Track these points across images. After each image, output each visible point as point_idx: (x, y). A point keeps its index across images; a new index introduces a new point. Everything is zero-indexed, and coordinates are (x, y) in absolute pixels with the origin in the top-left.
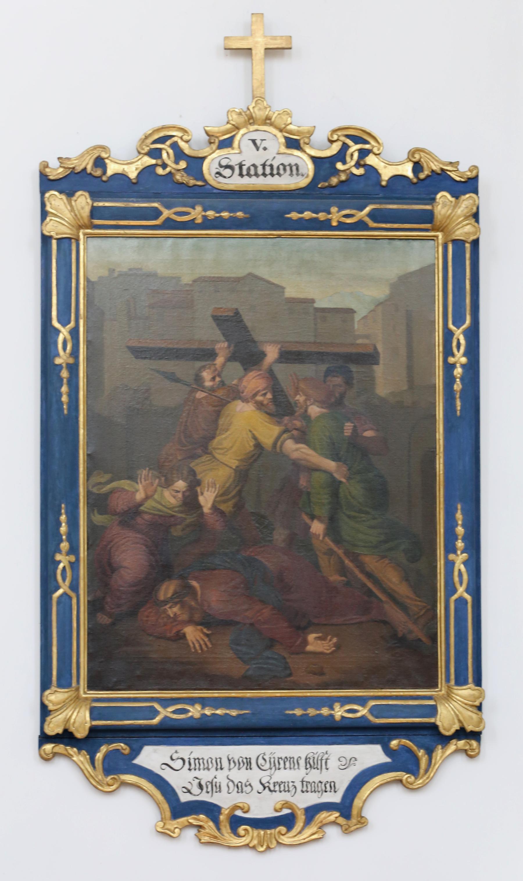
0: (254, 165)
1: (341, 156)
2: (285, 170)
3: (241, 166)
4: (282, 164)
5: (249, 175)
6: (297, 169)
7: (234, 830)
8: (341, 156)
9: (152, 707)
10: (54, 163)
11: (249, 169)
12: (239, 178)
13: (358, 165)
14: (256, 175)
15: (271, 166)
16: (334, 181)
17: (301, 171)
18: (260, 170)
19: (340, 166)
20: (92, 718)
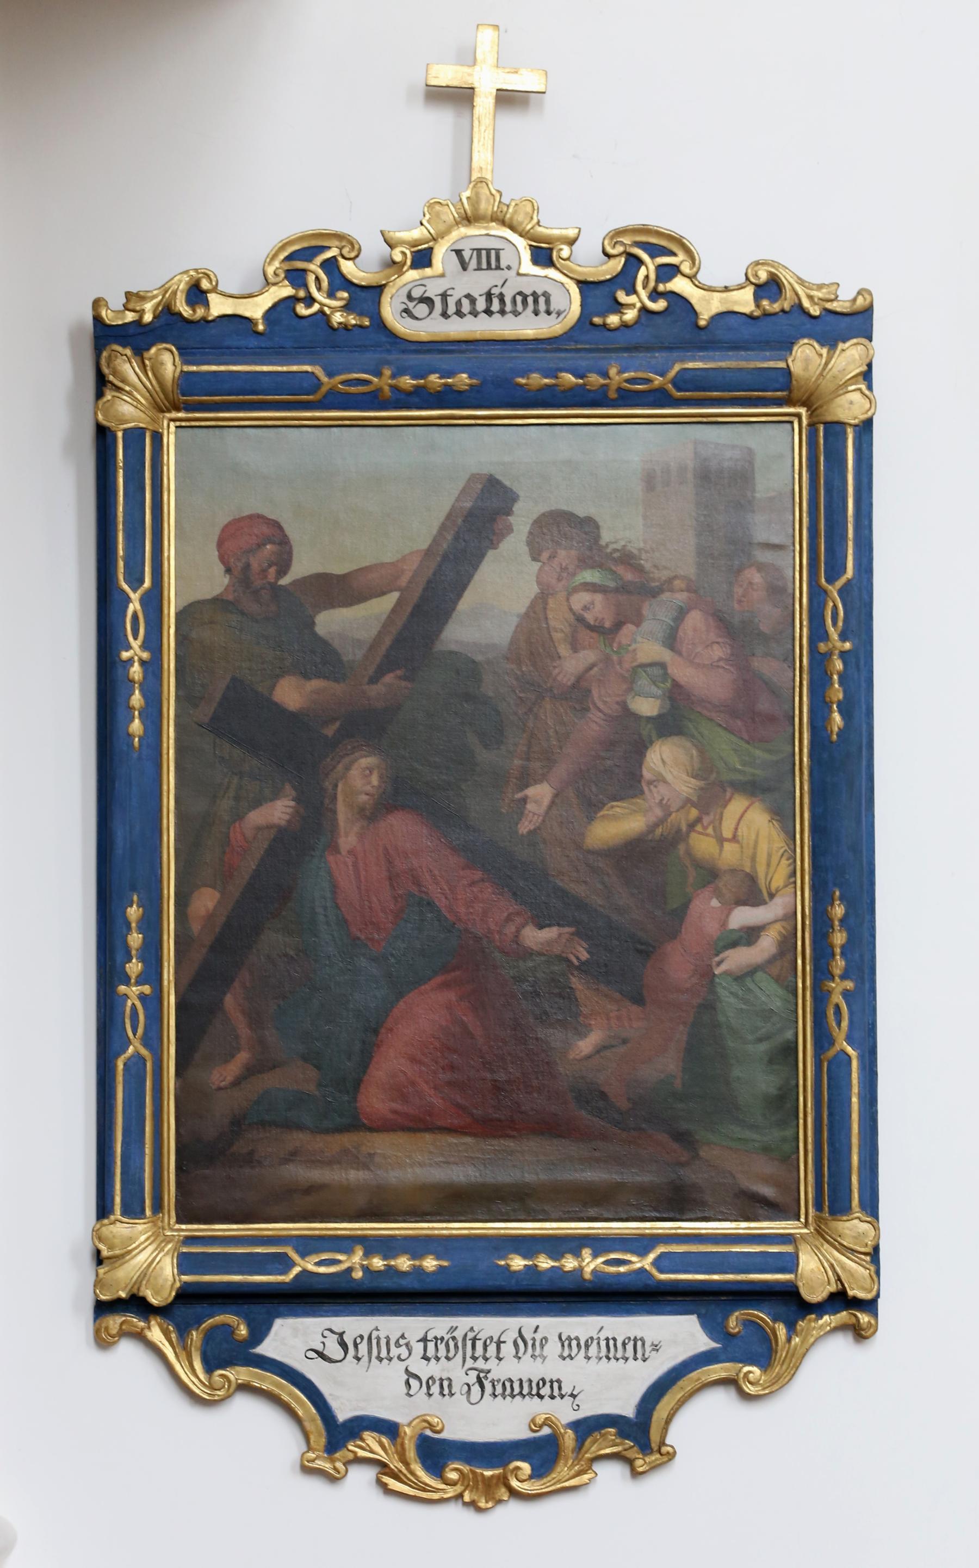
0: (468, 296)
1: (626, 280)
2: (525, 302)
4: (520, 293)
5: (459, 313)
6: (548, 302)
7: (436, 1469)
8: (626, 280)
9: (286, 1254)
10: (116, 301)
11: (459, 303)
12: (442, 319)
14: (474, 313)
15: (501, 298)
16: (613, 320)
17: (553, 307)
18: (481, 305)
19: (622, 297)
20: (182, 1271)
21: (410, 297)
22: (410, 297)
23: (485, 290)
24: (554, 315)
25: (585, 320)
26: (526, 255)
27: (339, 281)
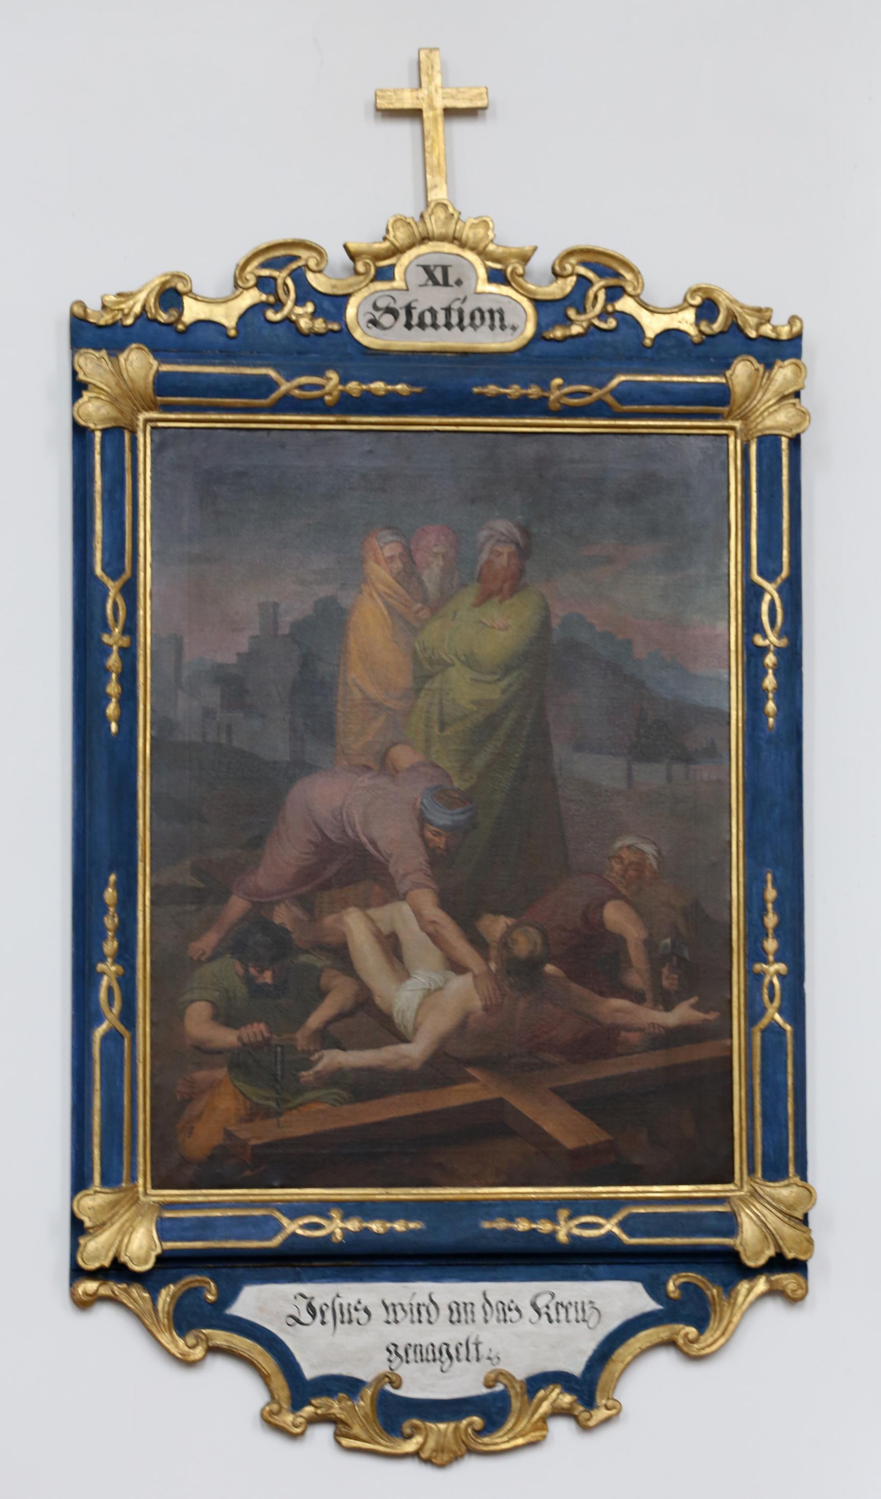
2: (483, 318)
3: (409, 309)
5: (422, 325)
6: (502, 319)
11: (421, 316)
12: (406, 330)
13: (604, 315)
14: (435, 326)
15: (461, 312)
17: (508, 321)
18: (441, 319)
19: (572, 313)
20: (162, 1238)
21: (375, 307)
22: (375, 307)
23: (445, 305)
24: (509, 331)
25: (539, 336)
26: (482, 273)
27: (305, 293)
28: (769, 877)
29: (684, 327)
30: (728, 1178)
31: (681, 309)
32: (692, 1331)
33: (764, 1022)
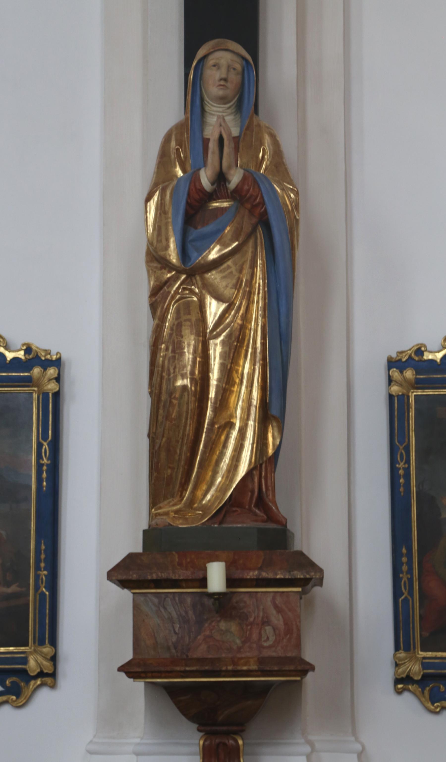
28: (43, 542)
29: (20, 356)
30: (26, 645)
31: (21, 350)
32: (14, 698)
33: (40, 591)
